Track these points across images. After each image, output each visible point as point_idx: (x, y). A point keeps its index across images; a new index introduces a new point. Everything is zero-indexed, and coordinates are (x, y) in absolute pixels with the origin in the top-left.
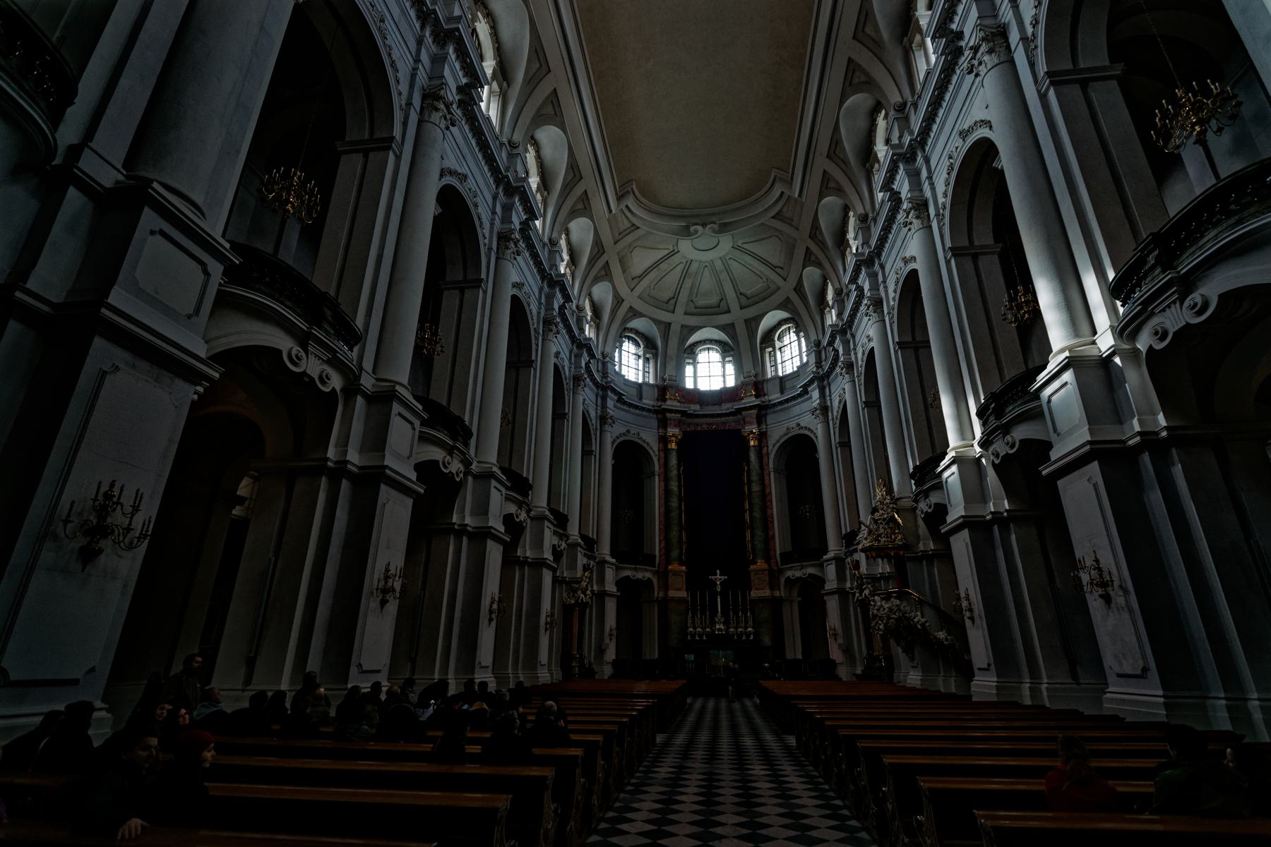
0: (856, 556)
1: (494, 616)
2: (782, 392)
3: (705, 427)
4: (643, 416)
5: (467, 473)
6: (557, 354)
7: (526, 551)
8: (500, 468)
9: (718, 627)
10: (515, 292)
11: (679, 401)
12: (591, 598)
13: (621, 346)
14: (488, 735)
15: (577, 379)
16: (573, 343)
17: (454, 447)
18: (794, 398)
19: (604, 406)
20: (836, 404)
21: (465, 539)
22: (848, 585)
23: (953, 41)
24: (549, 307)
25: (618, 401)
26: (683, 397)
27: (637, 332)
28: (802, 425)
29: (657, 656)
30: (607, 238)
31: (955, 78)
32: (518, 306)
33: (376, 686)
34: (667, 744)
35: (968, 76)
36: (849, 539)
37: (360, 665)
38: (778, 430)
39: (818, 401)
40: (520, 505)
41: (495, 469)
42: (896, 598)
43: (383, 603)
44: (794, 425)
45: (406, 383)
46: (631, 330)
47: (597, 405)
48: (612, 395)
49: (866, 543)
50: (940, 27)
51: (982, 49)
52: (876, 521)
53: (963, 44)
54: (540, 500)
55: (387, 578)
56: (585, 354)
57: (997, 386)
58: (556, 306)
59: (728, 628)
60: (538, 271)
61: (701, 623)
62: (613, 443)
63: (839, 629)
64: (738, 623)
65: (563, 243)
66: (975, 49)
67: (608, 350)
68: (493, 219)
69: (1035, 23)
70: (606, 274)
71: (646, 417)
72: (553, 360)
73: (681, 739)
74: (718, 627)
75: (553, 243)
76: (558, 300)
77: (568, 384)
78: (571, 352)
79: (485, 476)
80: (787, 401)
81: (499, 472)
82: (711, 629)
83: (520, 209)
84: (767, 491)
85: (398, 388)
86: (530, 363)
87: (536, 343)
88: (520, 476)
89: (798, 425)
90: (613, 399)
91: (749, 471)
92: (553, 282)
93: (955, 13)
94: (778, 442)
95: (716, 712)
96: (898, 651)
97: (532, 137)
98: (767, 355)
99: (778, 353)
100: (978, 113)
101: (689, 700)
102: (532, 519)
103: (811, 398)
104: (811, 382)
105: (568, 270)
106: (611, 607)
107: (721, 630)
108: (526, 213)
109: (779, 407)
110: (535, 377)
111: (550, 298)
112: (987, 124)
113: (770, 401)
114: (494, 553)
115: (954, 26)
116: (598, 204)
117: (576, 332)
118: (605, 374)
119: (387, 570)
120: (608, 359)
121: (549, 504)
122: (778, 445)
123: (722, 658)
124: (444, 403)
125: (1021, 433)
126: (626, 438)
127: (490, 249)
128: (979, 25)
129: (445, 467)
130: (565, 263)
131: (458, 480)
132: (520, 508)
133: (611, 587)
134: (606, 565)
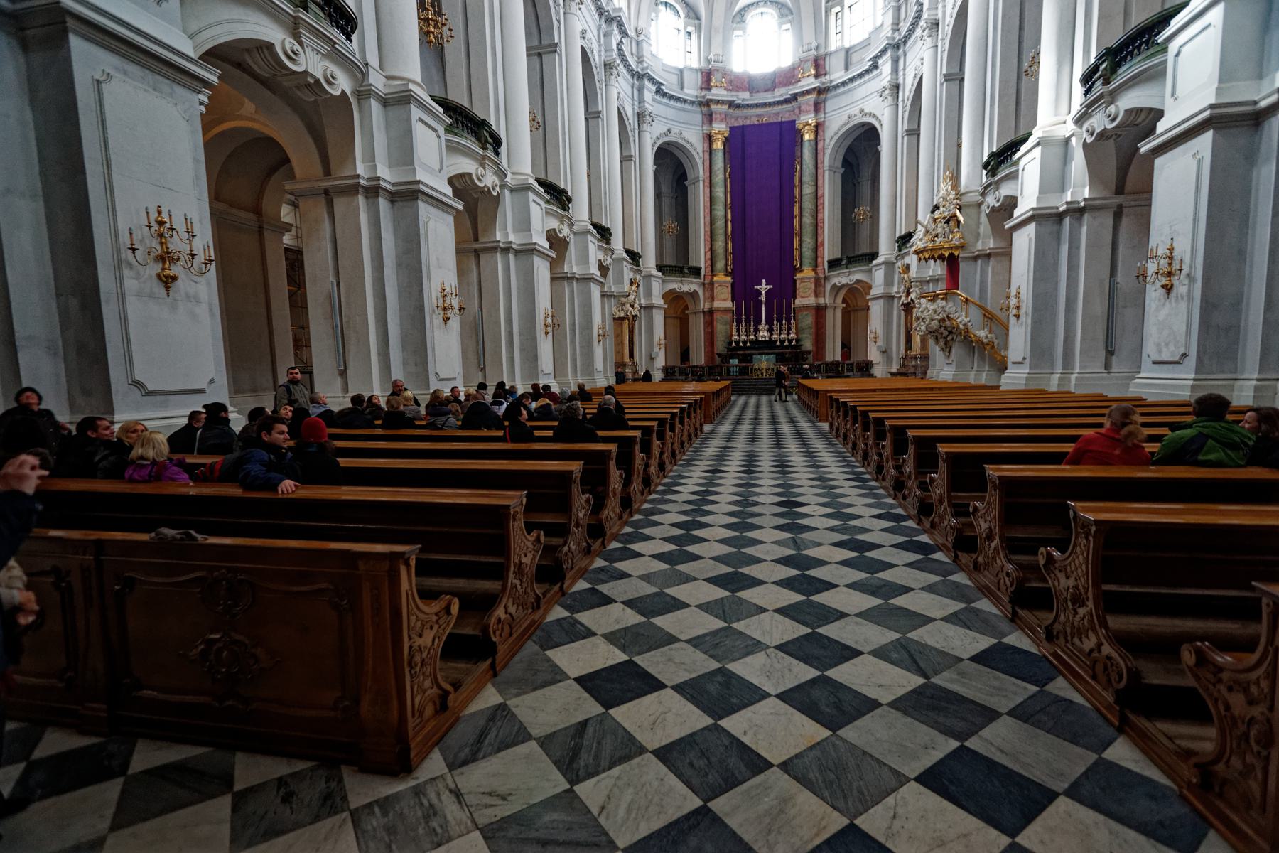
0: (907, 260)
1: (549, 329)
4: (684, 110)
5: (503, 186)
7: (572, 266)
9: (761, 334)
11: (726, 89)
12: (639, 311)
15: (608, 66)
17: (484, 157)
18: (860, 75)
19: (641, 101)
21: (511, 256)
22: (895, 289)
26: (731, 82)
28: (867, 111)
29: (703, 362)
33: (454, 389)
34: (712, 431)
36: (905, 239)
39: (889, 78)
42: (943, 299)
43: (446, 319)
45: (419, 79)
47: (633, 100)
49: (920, 245)
52: (935, 220)
57: (1115, 38)
59: (771, 334)
61: (746, 331)
62: (653, 146)
63: (880, 332)
67: (642, 25)
71: (688, 111)
72: (579, 42)
73: (725, 427)
77: (599, 73)
78: (599, 30)
80: (852, 80)
81: (536, 184)
82: (755, 335)
84: (820, 193)
85: (411, 86)
86: (553, 48)
89: (862, 111)
90: (650, 91)
94: (836, 134)
95: (758, 406)
96: (935, 350)
98: (833, 18)
101: (733, 398)
102: (575, 233)
103: (880, 74)
104: (884, 51)
106: (658, 318)
109: (842, 89)
113: (831, 81)
118: (640, 60)
120: (642, 37)
122: (836, 137)
123: (764, 362)
125: (1130, 100)
129: (479, 180)
131: (495, 194)
132: (562, 222)
133: (658, 300)
134: (652, 279)
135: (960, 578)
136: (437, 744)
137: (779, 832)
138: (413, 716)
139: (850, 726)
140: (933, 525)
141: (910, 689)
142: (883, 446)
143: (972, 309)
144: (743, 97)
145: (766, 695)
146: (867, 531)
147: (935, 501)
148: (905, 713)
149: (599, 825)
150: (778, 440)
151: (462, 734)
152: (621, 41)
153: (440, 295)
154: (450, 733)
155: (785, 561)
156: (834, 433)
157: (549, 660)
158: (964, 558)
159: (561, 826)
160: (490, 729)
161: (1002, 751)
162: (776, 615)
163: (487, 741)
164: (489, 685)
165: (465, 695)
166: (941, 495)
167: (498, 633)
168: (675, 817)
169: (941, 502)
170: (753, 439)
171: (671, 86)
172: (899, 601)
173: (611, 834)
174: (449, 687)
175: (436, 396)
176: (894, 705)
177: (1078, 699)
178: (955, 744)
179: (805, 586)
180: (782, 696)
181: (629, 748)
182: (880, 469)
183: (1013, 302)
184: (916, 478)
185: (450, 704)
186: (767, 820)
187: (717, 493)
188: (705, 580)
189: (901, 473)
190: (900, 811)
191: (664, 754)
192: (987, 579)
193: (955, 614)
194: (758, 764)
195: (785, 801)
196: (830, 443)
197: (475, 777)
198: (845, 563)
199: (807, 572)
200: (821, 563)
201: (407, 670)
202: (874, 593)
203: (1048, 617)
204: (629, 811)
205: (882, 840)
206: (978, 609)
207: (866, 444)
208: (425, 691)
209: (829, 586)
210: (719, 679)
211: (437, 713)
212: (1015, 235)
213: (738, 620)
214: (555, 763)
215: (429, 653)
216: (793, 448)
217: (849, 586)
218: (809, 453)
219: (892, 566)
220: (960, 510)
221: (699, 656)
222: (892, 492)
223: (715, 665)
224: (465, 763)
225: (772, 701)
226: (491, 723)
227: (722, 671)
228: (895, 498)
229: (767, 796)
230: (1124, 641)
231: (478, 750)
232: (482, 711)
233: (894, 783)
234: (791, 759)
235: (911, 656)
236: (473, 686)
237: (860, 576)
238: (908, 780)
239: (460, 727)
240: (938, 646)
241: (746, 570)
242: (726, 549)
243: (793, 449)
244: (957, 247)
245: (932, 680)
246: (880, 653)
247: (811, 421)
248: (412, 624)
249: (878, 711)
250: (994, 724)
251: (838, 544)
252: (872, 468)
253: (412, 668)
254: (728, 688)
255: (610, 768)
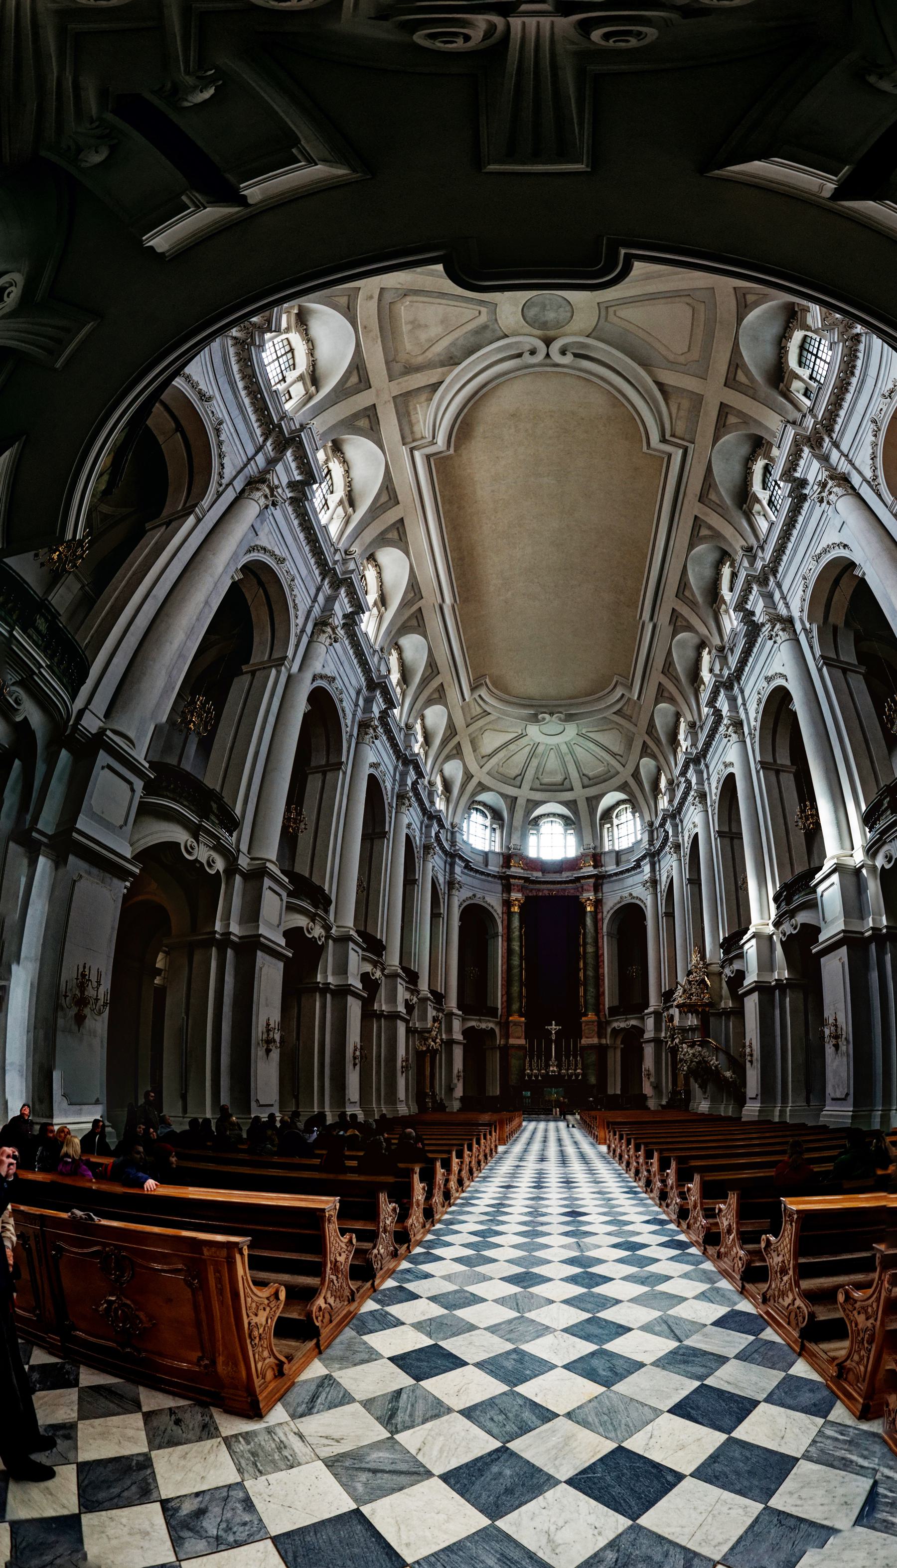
2: (618, 864)
3: (546, 893)
4: (489, 882)
5: (328, 937)
6: (409, 826)
8: (357, 932)
10: (372, 771)
11: (522, 869)
13: (469, 817)
14: (362, 1154)
15: (427, 848)
16: (424, 815)
17: (316, 914)
19: (452, 872)
20: (664, 878)
21: (328, 996)
24: (403, 783)
25: (465, 867)
26: (526, 864)
27: (485, 805)
28: (634, 895)
30: (459, 722)
32: (374, 783)
33: (272, 1117)
37: (257, 1101)
38: (613, 898)
40: (375, 964)
41: (352, 933)
43: (268, 1051)
44: (627, 895)
46: (479, 803)
48: (460, 862)
54: (393, 959)
55: (268, 1031)
56: (435, 825)
58: (409, 782)
60: (394, 752)
62: (460, 906)
64: (569, 1065)
65: (418, 727)
67: (456, 820)
68: (355, 711)
70: (457, 752)
71: (491, 882)
72: (405, 831)
74: (551, 1069)
75: (409, 727)
76: (412, 776)
77: (418, 852)
78: (422, 823)
79: (344, 939)
80: (622, 873)
81: (355, 935)
83: (381, 700)
86: (384, 835)
87: (390, 816)
88: (375, 938)
89: (631, 894)
90: (460, 866)
91: (585, 934)
92: (407, 761)
94: (611, 909)
95: (546, 1131)
97: (396, 644)
99: (615, 828)
105: (422, 750)
107: (554, 1071)
108: (386, 704)
109: (615, 878)
110: (388, 846)
111: (404, 775)
114: (354, 1008)
116: (453, 694)
117: (427, 805)
118: (453, 843)
119: (268, 1025)
120: (456, 829)
121: (401, 963)
122: (612, 912)
124: (307, 875)
126: (472, 902)
127: (351, 736)
129: (309, 933)
130: (419, 744)
131: (320, 943)
132: (375, 967)
135: (708, 1266)
136: (279, 1400)
137: (564, 1458)
138: (258, 1377)
139: (621, 1383)
140: (689, 1227)
141: (667, 1351)
142: (651, 1163)
143: (722, 1056)
144: (537, 875)
145: (553, 1367)
146: (639, 1234)
147: (690, 1207)
148: (664, 1368)
149: (417, 1461)
150: (563, 1160)
151: (299, 1395)
152: (439, 832)
153: (265, 1030)
154: (289, 1394)
155: (571, 1262)
156: (611, 1154)
157: (365, 1343)
158: (711, 1250)
159: (386, 1461)
160: (321, 1393)
161: (729, 1383)
162: (562, 1305)
163: (319, 1401)
164: (316, 1360)
165: (297, 1365)
166: (695, 1201)
167: (320, 1319)
168: (480, 1455)
169: (695, 1207)
170: (542, 1159)
171: (479, 865)
172: (663, 1287)
173: (427, 1466)
174: (283, 1359)
175: (257, 1118)
176: (656, 1364)
177: (778, 1340)
178: (697, 1384)
179: (587, 1281)
180: (567, 1367)
181: (438, 1410)
182: (648, 1183)
183: (748, 1050)
184: (677, 1188)
185: (286, 1372)
186: (554, 1452)
187: (510, 1206)
188: (501, 1279)
189: (666, 1186)
190: (655, 1433)
191: (468, 1413)
192: (726, 1264)
193: (703, 1293)
194: (546, 1415)
195: (568, 1438)
196: (608, 1162)
197: (312, 1425)
198: (621, 1261)
199: (589, 1270)
200: (600, 1261)
201: (248, 1341)
202: (643, 1283)
203: (764, 1287)
204: (441, 1451)
205: (641, 1453)
206: (719, 1288)
207: (638, 1163)
208: (265, 1359)
209: (607, 1279)
210: (514, 1356)
211: (275, 1377)
212: (746, 999)
213: (530, 1311)
214: (377, 1419)
215: (264, 1330)
216: (577, 1168)
217: (624, 1279)
218: (591, 1171)
219: (657, 1260)
220: (710, 1213)
221: (496, 1339)
222: (658, 1202)
223: (509, 1346)
224: (301, 1416)
225: (560, 1371)
226: (321, 1389)
227: (515, 1350)
228: (660, 1206)
229: (554, 1436)
230: (811, 1297)
231: (313, 1407)
232: (313, 1379)
233: (652, 1416)
234: (574, 1410)
235: (669, 1327)
236: (301, 1361)
237: (632, 1270)
238: (662, 1412)
239: (296, 1389)
240: (689, 1318)
241: (536, 1270)
242: (519, 1253)
243: (577, 1168)
244: (707, 1005)
245: (685, 1343)
246: (647, 1328)
247: (592, 1144)
248: (248, 1305)
249: (643, 1370)
250: (724, 1366)
251: (615, 1246)
252: (641, 1183)
253: (252, 1340)
254: (522, 1363)
255: (423, 1423)
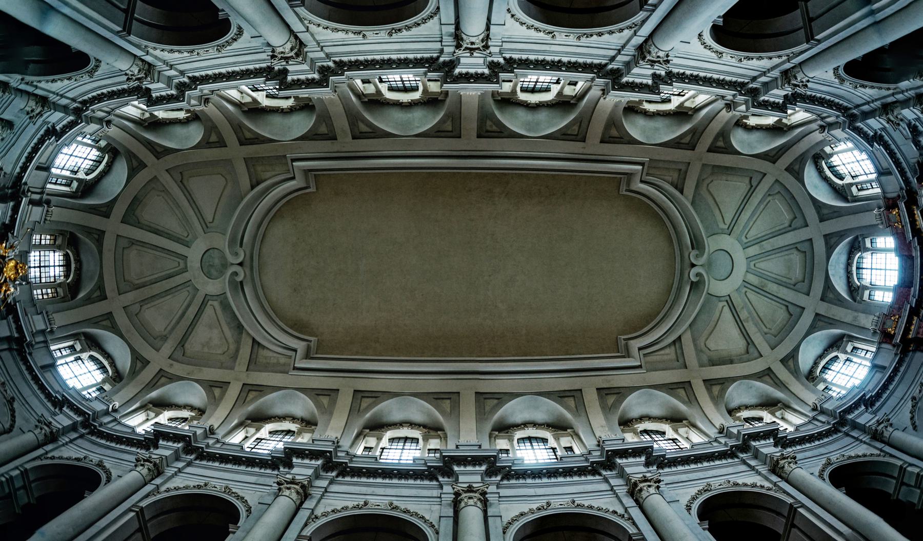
23: (789, 100)
31: (809, 93)
35: (809, 86)
50: (782, 110)
51: (795, 82)
53: (790, 93)
66: (796, 86)
69: (780, 57)
93: (774, 103)
100: (830, 76)
112: (836, 69)
115: (781, 101)
128: (781, 87)
